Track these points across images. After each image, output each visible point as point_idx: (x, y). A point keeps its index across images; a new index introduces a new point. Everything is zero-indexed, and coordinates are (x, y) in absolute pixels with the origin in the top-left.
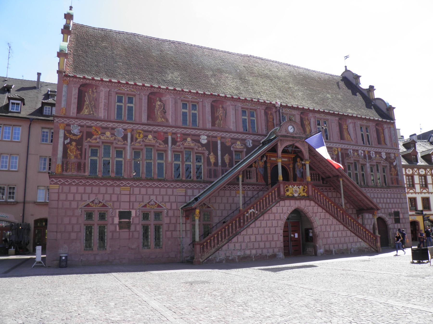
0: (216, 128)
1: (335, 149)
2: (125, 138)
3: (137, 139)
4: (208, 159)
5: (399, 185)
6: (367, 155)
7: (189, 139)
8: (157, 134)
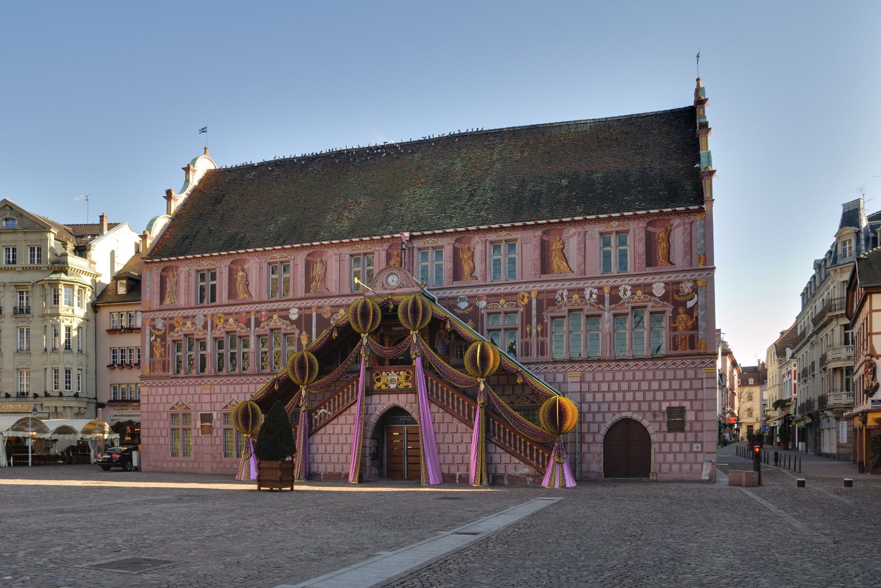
0: (312, 294)
1: (523, 296)
2: (205, 327)
3: (217, 325)
4: (299, 340)
5: (695, 351)
6: (607, 296)
7: (275, 317)
8: (238, 315)
